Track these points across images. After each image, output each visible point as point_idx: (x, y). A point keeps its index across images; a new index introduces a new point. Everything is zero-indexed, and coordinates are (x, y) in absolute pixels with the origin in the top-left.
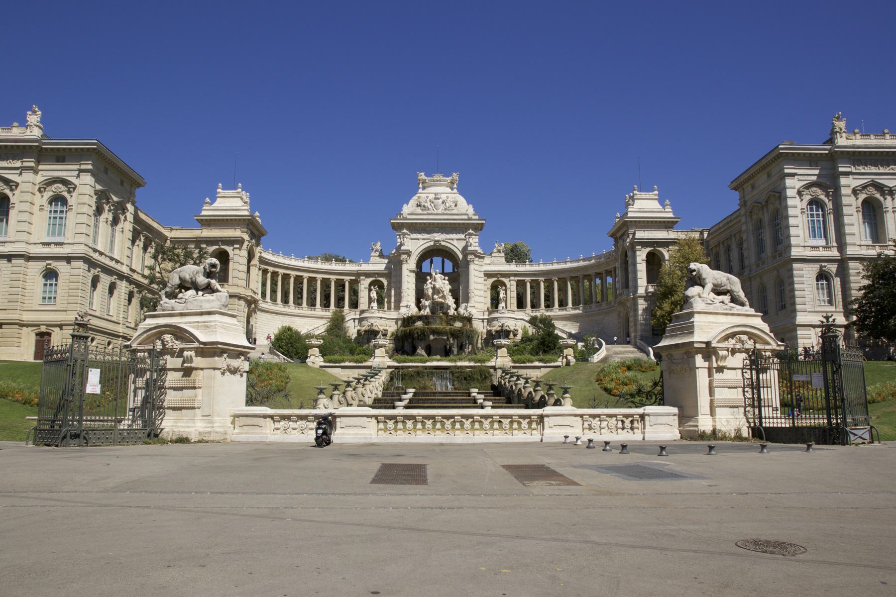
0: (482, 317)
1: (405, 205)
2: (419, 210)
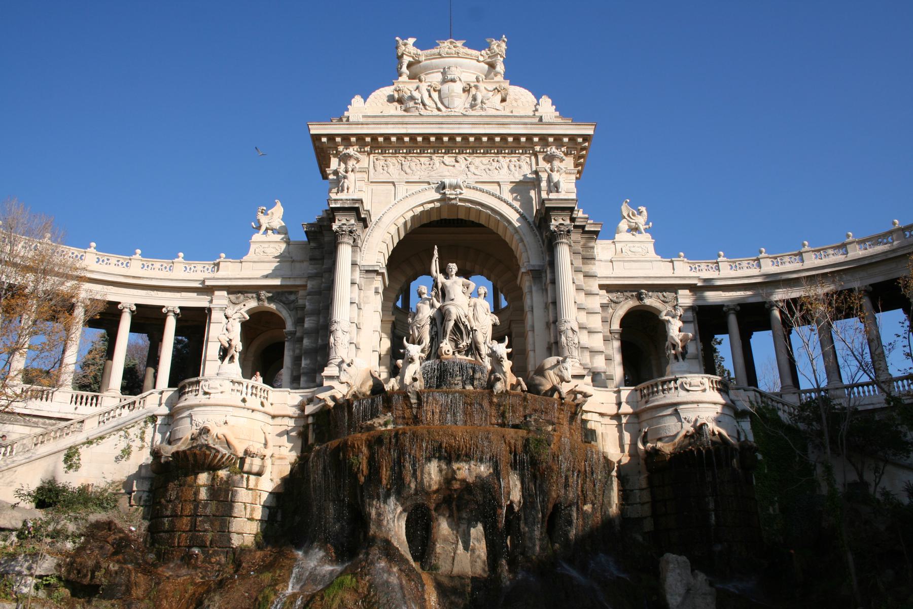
0: (613, 410)
1: (357, 101)
2: (394, 109)
